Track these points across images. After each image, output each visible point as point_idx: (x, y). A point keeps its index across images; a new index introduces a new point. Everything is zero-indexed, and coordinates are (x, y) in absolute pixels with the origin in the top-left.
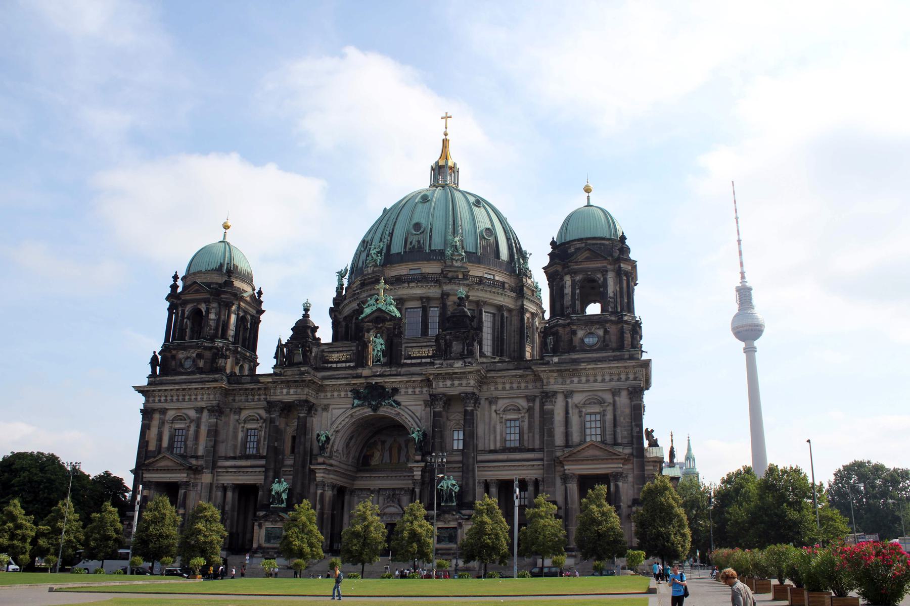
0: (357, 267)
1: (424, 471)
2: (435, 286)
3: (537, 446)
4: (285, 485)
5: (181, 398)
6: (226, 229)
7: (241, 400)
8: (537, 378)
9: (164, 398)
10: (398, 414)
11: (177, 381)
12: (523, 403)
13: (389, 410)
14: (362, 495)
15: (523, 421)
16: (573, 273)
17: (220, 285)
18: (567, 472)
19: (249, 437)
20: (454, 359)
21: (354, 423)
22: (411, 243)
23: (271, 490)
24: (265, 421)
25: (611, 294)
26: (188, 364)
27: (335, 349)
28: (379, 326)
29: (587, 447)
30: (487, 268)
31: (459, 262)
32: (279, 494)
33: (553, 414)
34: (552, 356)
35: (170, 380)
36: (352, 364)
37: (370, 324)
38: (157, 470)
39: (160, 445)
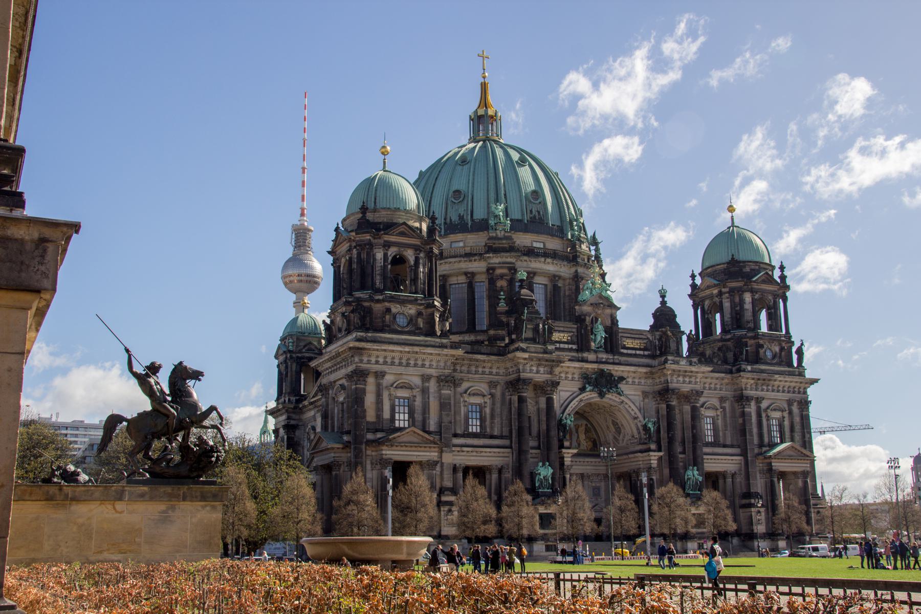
0: (445, 219)
1: (660, 459)
3: (728, 442)
4: (551, 471)
6: (385, 155)
10: (622, 402)
11: (394, 341)
16: (752, 291)
18: (774, 468)
22: (531, 211)
23: (540, 474)
24: (492, 396)
26: (401, 321)
33: (751, 417)
34: (747, 365)
35: (385, 338)
36: (574, 347)
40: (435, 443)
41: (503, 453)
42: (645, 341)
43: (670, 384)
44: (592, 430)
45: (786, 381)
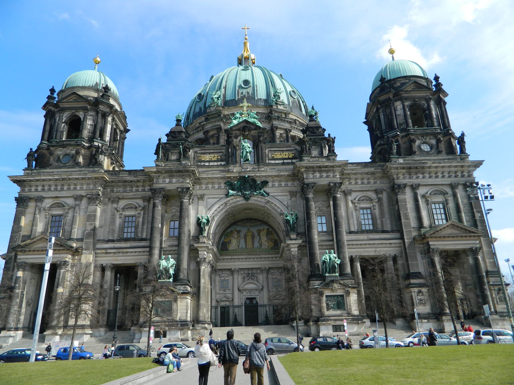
0: (194, 113)
1: (300, 247)
2: (266, 121)
3: (388, 227)
4: (172, 261)
5: (59, 188)
7: (120, 191)
8: (386, 175)
9: (42, 188)
10: (268, 202)
12: (373, 195)
13: (259, 199)
14: (223, 275)
15: (374, 209)
16: (402, 100)
17: (96, 98)
18: (432, 247)
19: (126, 224)
20: (318, 157)
21: (226, 211)
22: (242, 93)
23: (159, 266)
25: (435, 116)
27: (207, 151)
28: (246, 133)
29: (448, 226)
30: (296, 116)
31: (282, 106)
32: (167, 270)
34: (398, 158)
35: (47, 172)
37: (238, 132)
38: (34, 251)
39: (36, 229)
40: (61, 246)
41: (144, 252)
42: (294, 152)
43: (305, 180)
44: (273, 232)
45: (443, 167)
